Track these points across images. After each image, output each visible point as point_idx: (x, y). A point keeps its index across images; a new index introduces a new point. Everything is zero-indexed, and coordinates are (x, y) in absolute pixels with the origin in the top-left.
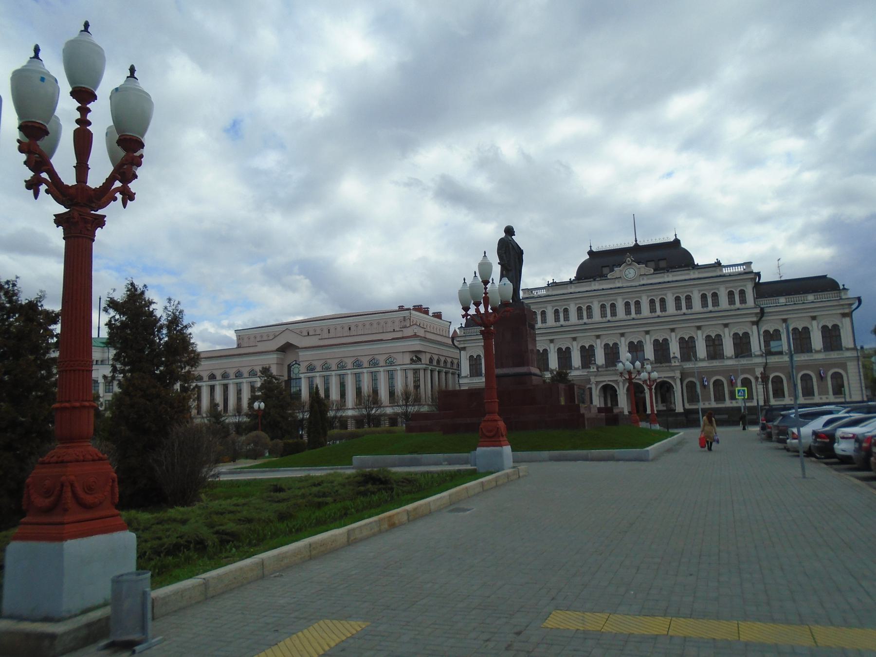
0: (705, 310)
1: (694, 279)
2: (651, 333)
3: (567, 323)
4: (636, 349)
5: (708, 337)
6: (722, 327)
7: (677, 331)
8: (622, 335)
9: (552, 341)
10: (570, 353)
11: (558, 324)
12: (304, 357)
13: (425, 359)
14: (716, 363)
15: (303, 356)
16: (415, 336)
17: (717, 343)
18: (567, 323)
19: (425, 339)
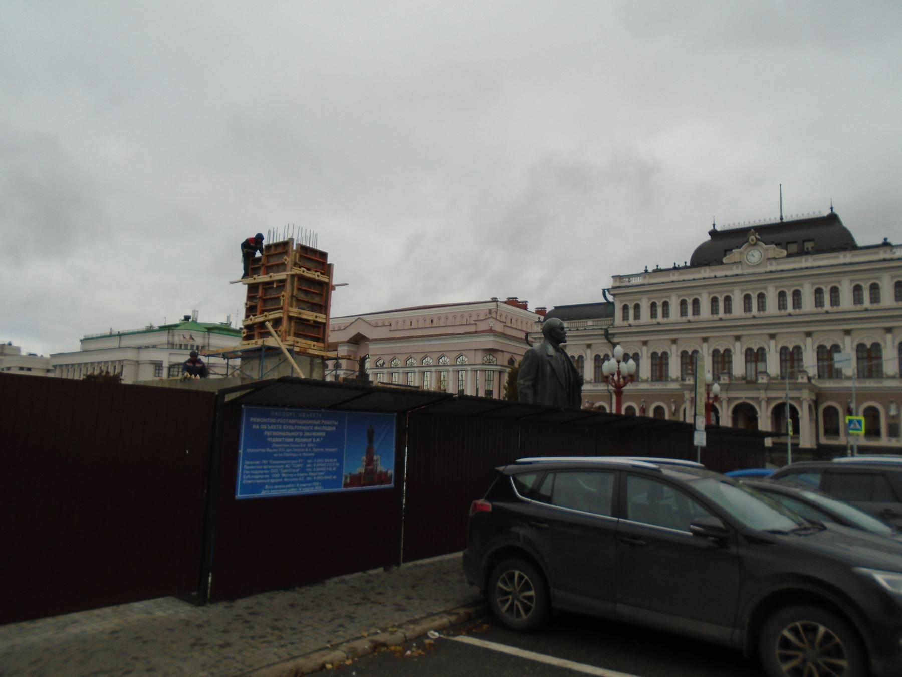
0: (859, 307)
1: (844, 264)
2: (743, 339)
3: (666, 320)
4: (755, 356)
5: (784, 350)
6: (767, 338)
7: (815, 336)
8: (738, 338)
9: (645, 343)
10: (667, 358)
11: (654, 321)
12: (373, 349)
13: (503, 359)
14: (870, 384)
15: (373, 349)
16: (491, 331)
17: (796, 357)
18: (666, 320)
19: (503, 335)
